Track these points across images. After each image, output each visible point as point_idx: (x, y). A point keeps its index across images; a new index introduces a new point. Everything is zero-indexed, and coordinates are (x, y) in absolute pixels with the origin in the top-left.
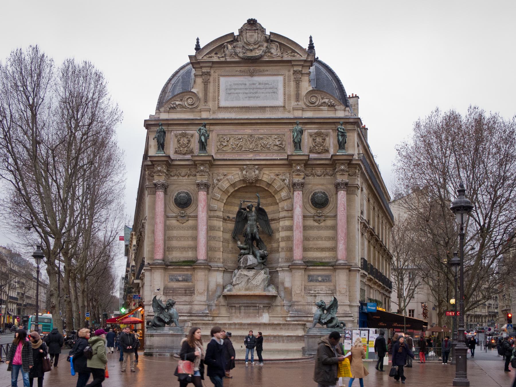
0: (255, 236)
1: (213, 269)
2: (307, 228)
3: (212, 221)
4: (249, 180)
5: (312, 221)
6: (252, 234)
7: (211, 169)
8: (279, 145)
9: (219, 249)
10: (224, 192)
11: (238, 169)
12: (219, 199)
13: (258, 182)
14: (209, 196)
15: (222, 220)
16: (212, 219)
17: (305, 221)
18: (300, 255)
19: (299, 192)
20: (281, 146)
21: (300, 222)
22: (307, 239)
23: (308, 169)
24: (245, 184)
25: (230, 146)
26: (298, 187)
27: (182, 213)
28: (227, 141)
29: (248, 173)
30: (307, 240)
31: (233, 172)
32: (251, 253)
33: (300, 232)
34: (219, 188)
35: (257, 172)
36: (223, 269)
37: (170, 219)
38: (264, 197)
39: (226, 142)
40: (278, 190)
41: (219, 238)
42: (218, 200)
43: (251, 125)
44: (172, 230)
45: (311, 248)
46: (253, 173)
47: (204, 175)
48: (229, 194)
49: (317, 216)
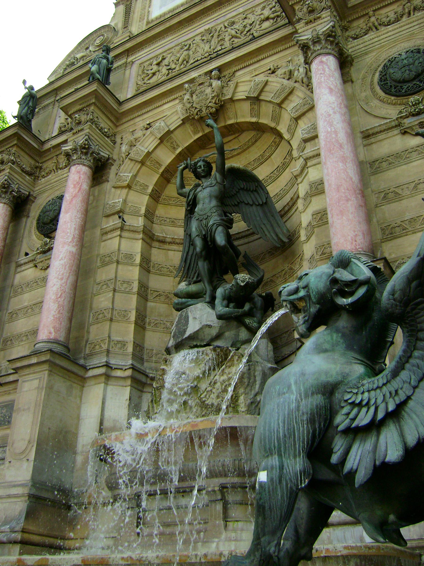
0: (213, 240)
1: (91, 373)
2: (384, 164)
3: (109, 241)
4: (200, 110)
5: (399, 137)
6: (204, 238)
7: (119, 129)
8: (272, 16)
9: (124, 315)
10: (142, 163)
11: (177, 101)
12: (126, 183)
13: (231, 113)
14: (107, 186)
15: (141, 236)
16: (109, 236)
17: (374, 146)
18: (352, 234)
19: (324, 59)
20: (275, 14)
21: (336, 132)
22: (391, 195)
23: (355, 24)
24: (199, 132)
25: (164, 70)
26: (318, 47)
27: (46, 244)
28: (158, 64)
29: (194, 96)
30: (390, 202)
31: (165, 115)
32: (208, 299)
33: (344, 159)
34: (132, 160)
35: (216, 83)
36: (129, 373)
37: (23, 268)
38: (262, 156)
39: (155, 68)
40: (278, 101)
41: (129, 283)
42: (129, 187)
43: (209, 15)
44: (22, 293)
45: (412, 220)
46: (208, 90)
47: (82, 130)
48: (161, 171)
49: (413, 115)
